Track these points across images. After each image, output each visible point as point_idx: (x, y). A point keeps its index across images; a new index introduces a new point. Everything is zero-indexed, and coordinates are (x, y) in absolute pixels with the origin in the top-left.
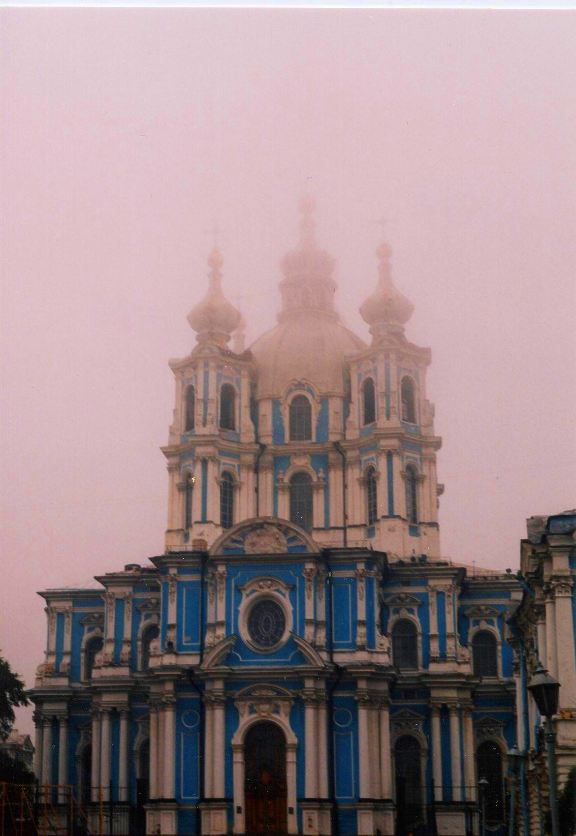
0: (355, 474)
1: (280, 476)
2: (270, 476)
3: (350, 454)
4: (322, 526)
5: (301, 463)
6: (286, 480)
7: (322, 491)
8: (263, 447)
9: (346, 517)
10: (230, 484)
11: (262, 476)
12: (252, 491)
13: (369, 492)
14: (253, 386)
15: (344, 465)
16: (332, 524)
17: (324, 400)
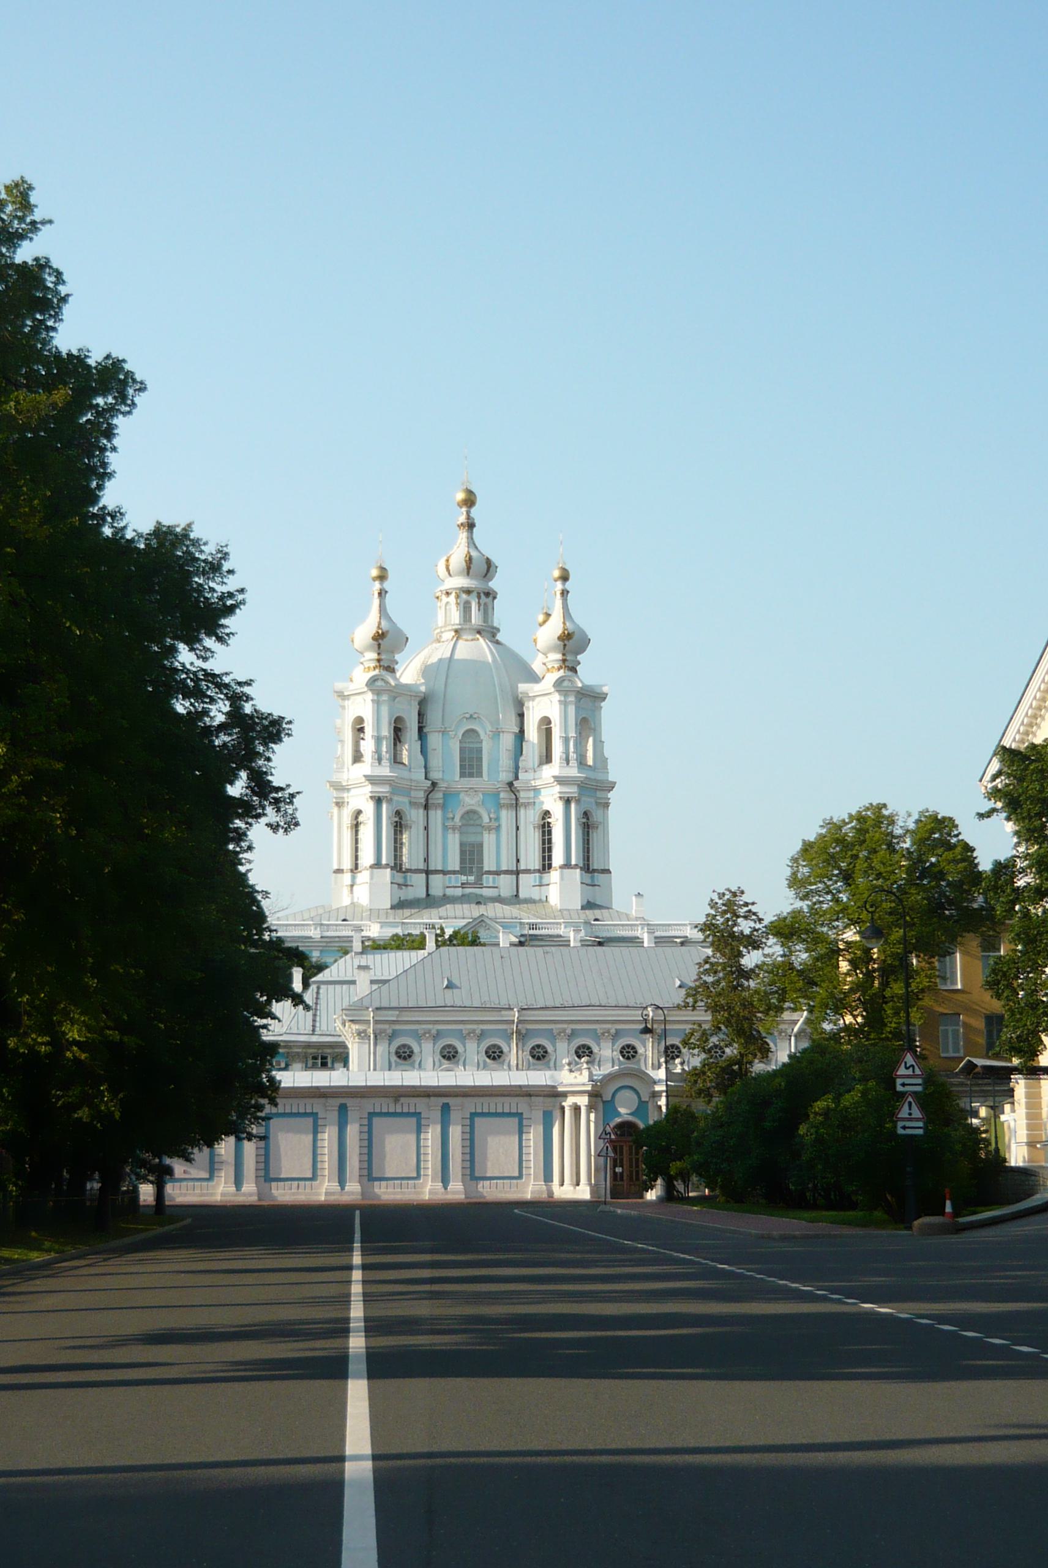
0: (529, 818)
1: (451, 816)
2: (439, 812)
3: (522, 795)
4: (494, 869)
5: (470, 801)
6: (457, 819)
7: (494, 831)
8: (434, 784)
9: (518, 861)
10: (400, 822)
11: (432, 813)
12: (422, 828)
13: (543, 835)
14: (421, 715)
15: (516, 805)
16: (504, 868)
17: (497, 734)
